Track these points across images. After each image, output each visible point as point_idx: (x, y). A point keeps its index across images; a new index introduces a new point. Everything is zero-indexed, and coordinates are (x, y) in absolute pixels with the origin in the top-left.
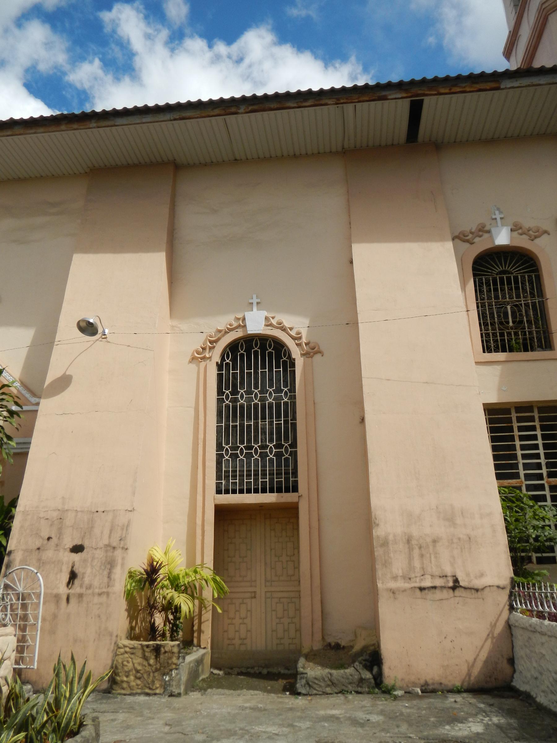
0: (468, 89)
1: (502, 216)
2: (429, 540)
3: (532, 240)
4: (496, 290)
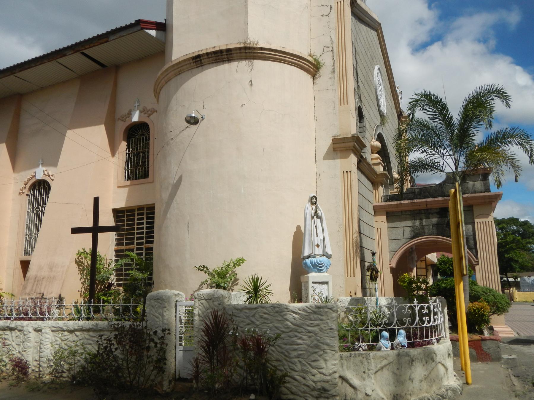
0: (96, 44)
1: (138, 104)
2: (42, 277)
3: (148, 117)
4: (137, 145)
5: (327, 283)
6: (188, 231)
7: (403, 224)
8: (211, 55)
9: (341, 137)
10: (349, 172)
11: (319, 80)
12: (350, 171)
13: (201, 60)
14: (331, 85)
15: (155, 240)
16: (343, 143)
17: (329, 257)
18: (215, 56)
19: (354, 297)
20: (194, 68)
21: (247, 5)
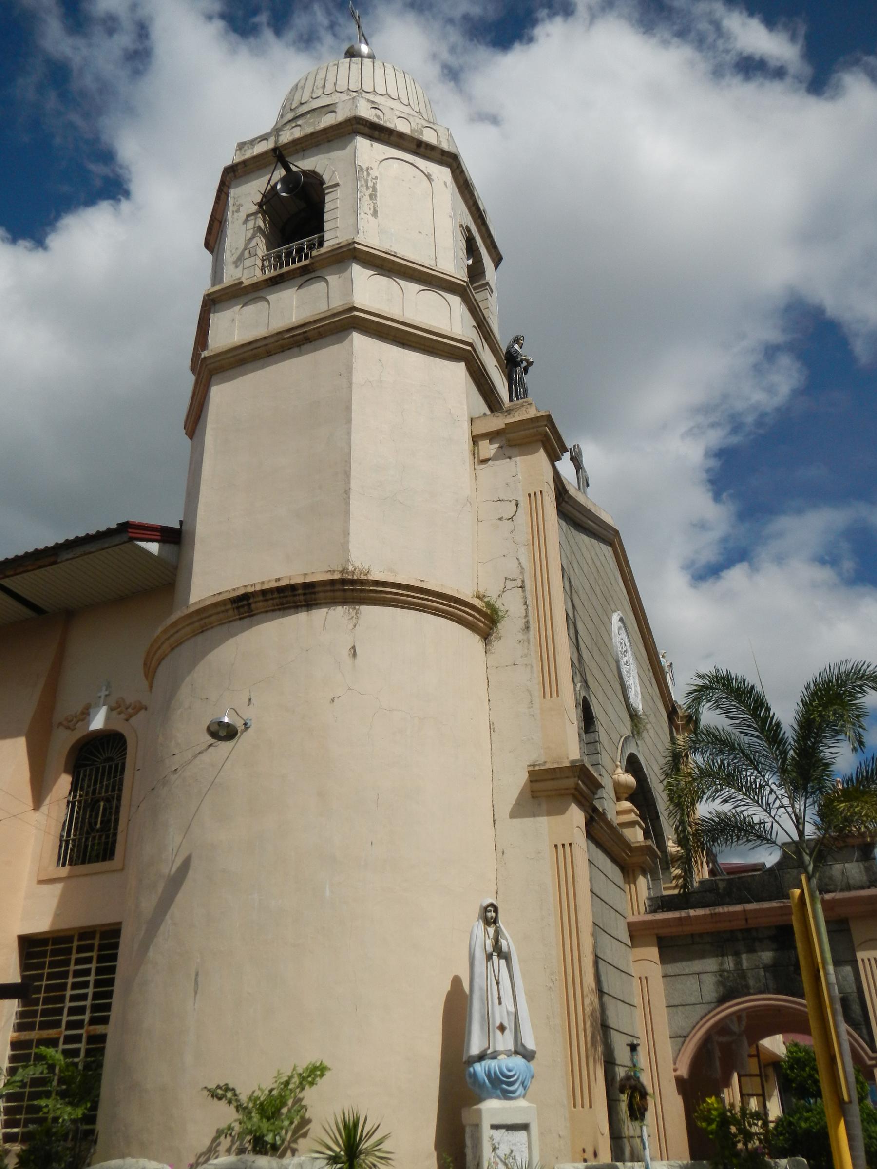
1: (107, 693)
3: (127, 720)
4: (95, 783)
5: (525, 1127)
6: (196, 993)
7: (697, 965)
8: (272, 594)
9: (548, 766)
10: (567, 847)
11: (497, 646)
12: (570, 844)
13: (249, 605)
14: (522, 656)
15: (114, 1014)
16: (553, 779)
17: (529, 1056)
18: (280, 597)
19: (592, 1162)
20: (235, 620)
21: (349, 498)
